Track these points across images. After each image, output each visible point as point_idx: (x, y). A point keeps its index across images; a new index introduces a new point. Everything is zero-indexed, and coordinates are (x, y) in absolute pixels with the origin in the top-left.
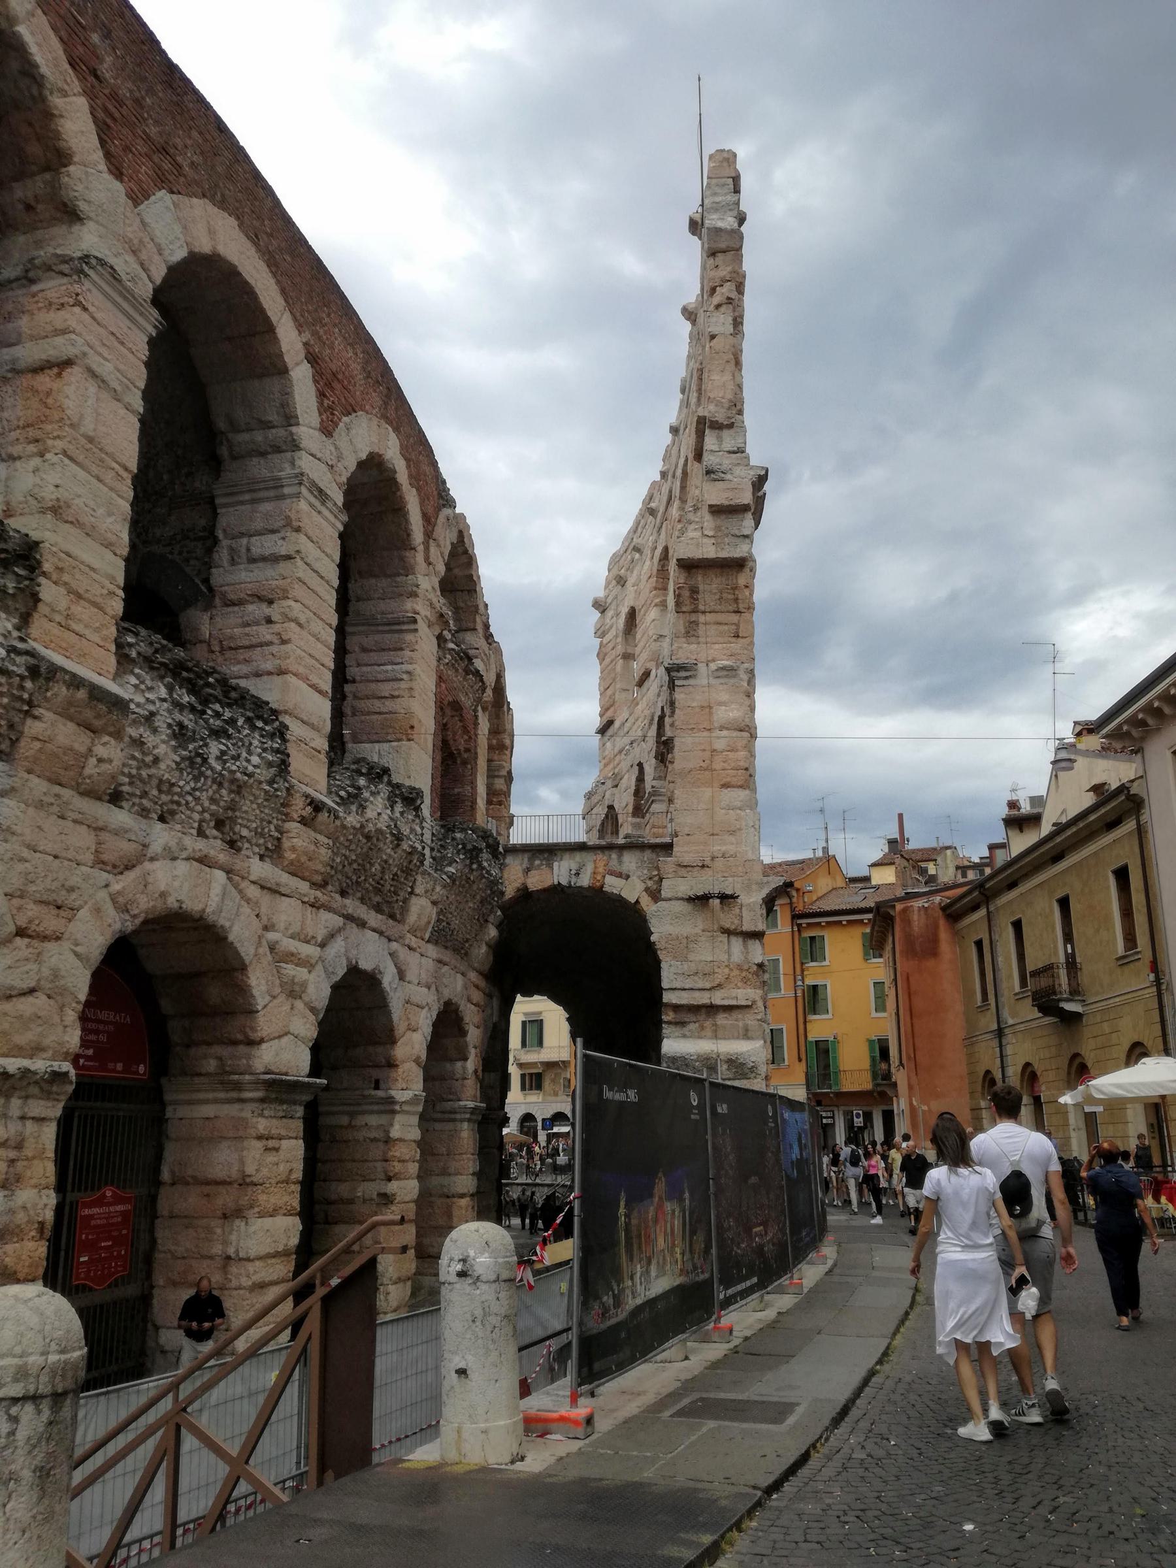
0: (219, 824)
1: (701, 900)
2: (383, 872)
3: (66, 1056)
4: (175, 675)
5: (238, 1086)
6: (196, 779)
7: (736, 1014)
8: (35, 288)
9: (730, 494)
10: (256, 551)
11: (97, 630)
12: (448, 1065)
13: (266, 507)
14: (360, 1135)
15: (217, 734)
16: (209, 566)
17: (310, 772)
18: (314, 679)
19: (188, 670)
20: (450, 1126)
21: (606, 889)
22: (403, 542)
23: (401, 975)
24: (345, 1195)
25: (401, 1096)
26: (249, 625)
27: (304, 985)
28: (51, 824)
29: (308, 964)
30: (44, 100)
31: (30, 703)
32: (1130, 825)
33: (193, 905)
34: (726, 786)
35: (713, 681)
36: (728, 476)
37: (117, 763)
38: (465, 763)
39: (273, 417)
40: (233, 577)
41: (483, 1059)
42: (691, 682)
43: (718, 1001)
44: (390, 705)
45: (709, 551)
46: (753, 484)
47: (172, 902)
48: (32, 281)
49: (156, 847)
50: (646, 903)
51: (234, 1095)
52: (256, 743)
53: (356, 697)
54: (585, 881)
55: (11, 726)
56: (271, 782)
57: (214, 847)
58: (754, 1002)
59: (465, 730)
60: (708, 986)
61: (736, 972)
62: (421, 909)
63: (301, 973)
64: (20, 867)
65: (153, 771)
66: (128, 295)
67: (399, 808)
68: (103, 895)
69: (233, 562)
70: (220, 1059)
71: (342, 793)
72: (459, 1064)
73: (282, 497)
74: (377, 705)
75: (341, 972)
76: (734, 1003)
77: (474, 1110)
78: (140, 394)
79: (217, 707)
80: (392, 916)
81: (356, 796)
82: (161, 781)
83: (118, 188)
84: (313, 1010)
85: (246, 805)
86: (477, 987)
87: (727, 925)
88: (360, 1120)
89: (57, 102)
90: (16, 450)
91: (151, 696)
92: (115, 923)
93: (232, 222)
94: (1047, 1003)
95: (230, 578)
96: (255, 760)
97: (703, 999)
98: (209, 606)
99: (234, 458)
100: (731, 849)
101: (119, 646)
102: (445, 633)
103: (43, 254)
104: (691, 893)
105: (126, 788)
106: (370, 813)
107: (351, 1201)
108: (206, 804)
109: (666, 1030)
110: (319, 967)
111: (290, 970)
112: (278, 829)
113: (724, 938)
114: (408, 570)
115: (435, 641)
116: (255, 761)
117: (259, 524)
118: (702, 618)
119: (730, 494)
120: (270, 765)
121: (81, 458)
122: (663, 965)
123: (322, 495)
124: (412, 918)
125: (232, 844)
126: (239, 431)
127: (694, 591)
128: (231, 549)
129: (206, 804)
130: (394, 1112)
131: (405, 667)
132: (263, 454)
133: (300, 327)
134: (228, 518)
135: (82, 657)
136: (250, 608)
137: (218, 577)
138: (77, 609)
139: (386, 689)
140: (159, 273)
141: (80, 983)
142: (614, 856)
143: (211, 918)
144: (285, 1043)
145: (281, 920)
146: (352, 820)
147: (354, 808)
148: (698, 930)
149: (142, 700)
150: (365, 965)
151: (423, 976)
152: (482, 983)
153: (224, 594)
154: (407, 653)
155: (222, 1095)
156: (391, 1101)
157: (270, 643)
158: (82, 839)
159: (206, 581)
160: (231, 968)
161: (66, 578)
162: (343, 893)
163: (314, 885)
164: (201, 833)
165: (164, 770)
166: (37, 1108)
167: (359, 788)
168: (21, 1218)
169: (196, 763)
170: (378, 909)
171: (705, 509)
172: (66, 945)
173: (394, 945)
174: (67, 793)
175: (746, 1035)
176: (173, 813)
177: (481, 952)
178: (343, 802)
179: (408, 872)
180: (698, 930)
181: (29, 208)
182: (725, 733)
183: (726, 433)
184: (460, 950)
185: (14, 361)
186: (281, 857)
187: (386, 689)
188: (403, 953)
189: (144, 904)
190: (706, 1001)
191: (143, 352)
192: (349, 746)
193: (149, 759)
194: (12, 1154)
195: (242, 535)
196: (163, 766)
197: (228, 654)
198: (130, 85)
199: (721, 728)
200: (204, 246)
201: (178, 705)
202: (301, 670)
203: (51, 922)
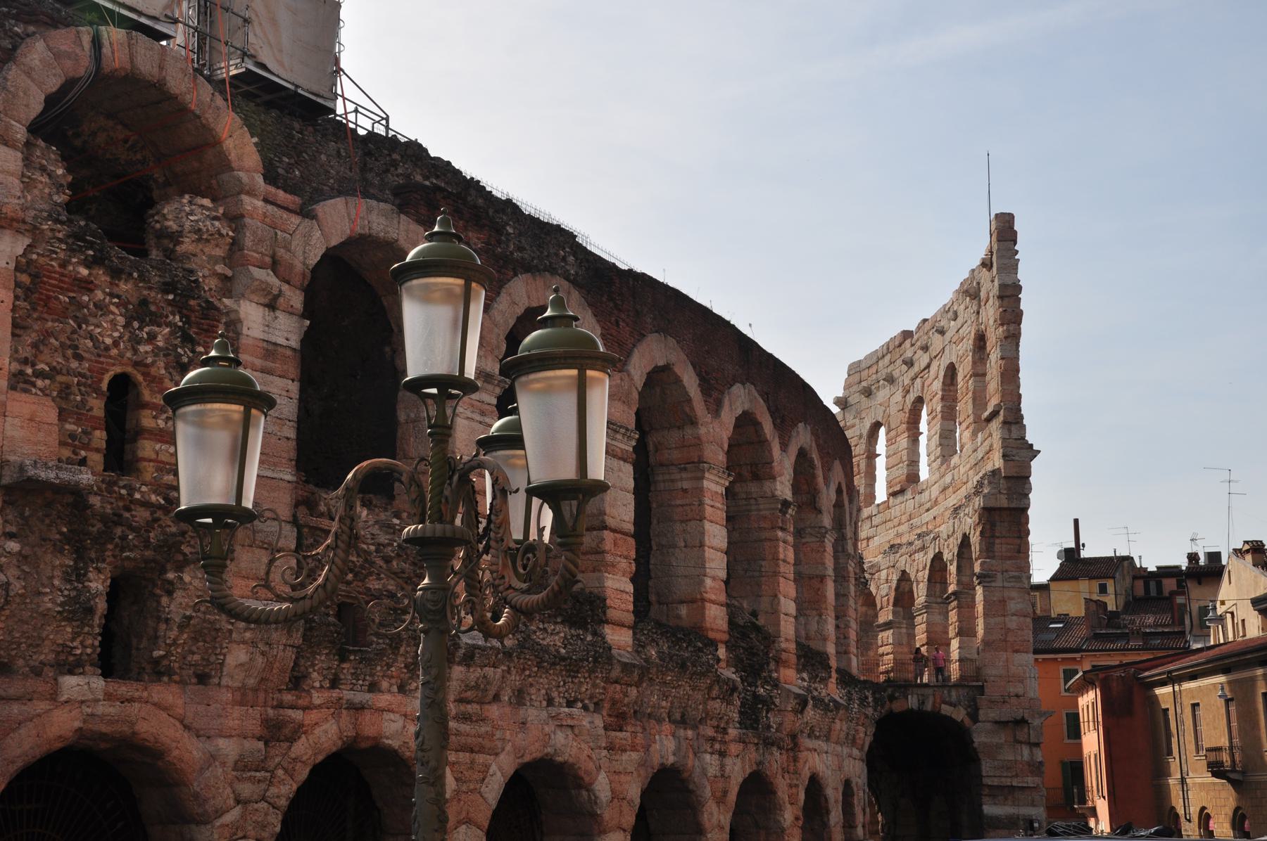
21: (943, 712)
34: (1017, 651)
43: (1015, 784)
50: (967, 722)
97: (1007, 782)
100: (1020, 691)
104: (997, 719)
109: (985, 799)
118: (997, 541)
148: (1002, 741)
175: (1033, 805)
199: (1013, 615)
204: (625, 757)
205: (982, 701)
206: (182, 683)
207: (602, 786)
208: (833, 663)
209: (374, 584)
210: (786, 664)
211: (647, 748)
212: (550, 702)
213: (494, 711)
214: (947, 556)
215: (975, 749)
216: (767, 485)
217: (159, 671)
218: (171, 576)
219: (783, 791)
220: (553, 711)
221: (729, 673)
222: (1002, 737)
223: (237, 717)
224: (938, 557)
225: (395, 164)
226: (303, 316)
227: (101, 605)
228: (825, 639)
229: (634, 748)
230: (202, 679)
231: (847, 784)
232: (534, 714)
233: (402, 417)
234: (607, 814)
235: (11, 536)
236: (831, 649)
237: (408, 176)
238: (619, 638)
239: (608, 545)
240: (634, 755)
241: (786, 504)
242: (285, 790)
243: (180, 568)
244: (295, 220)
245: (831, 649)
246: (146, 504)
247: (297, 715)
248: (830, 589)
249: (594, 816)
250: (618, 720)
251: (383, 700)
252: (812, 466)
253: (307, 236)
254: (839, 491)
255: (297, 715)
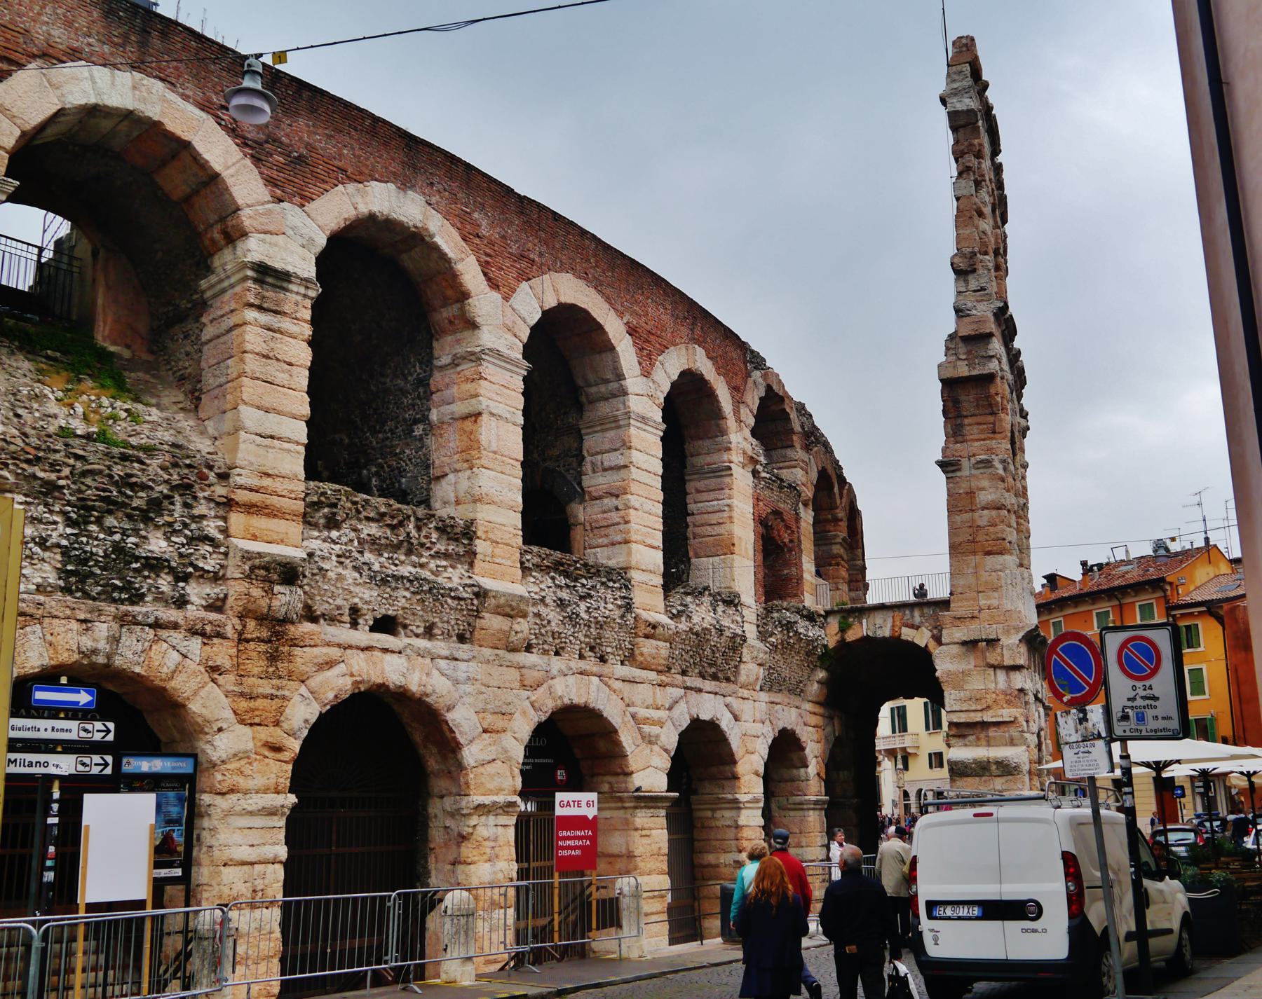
0: (592, 649)
1: (970, 645)
2: (714, 653)
3: (515, 792)
4: (556, 570)
5: (621, 800)
6: (574, 626)
7: (1003, 728)
8: (459, 369)
9: (975, 326)
10: (606, 464)
11: (509, 558)
12: (795, 771)
13: (611, 434)
14: (719, 823)
15: (582, 598)
16: (580, 474)
17: (650, 602)
18: (649, 541)
19: (562, 565)
20: (801, 813)
21: (903, 637)
22: (718, 414)
23: (736, 718)
24: (713, 862)
25: (742, 797)
26: (605, 512)
27: (658, 736)
28: (496, 671)
29: (660, 724)
30: (452, 268)
31: (477, 611)
33: (579, 700)
34: (989, 553)
35: (974, 472)
36: (974, 312)
37: (526, 631)
38: (790, 551)
39: (609, 376)
40: (594, 481)
41: (826, 765)
42: (958, 474)
44: (718, 530)
46: (995, 315)
47: (566, 701)
48: (457, 365)
49: (554, 672)
51: (620, 805)
52: (609, 596)
53: (695, 526)
54: (886, 632)
55: (469, 625)
56: (622, 617)
57: (591, 664)
58: (1016, 718)
59: (787, 527)
60: (979, 708)
61: (1001, 697)
62: (750, 670)
63: (655, 730)
64: (482, 697)
65: (548, 628)
66: (508, 360)
67: (720, 608)
68: (527, 703)
69: (594, 472)
70: (610, 783)
71: (674, 611)
72: (802, 770)
73: (619, 427)
74: (709, 530)
75: (686, 723)
76: (1000, 719)
77: (816, 802)
78: (521, 413)
79: (584, 581)
80: (728, 680)
81: (683, 611)
82: (553, 633)
83: (496, 296)
84: (666, 751)
85: (607, 634)
86: (815, 714)
87: (992, 662)
88: (718, 814)
89: (459, 267)
90: (458, 466)
91: (543, 586)
92: (535, 718)
93: (570, 276)
95: (593, 482)
96: (610, 606)
97: (977, 717)
98: (582, 501)
99: (591, 402)
100: (994, 602)
101: (522, 563)
102: (759, 467)
103: (460, 350)
105: (534, 641)
106: (696, 619)
107: (717, 866)
108: (583, 639)
110: (669, 724)
111: (647, 729)
112: (630, 643)
113: (991, 671)
114: (723, 432)
115: (750, 475)
116: (609, 607)
117: (607, 446)
118: (966, 421)
119: (975, 326)
120: (620, 607)
121: (491, 466)
122: (946, 694)
123: (644, 420)
124: (743, 678)
125: (603, 659)
126: (591, 386)
128: (592, 463)
129: (583, 639)
130: (740, 808)
131: (727, 502)
132: (607, 399)
133: (621, 314)
134: (590, 442)
135: (502, 576)
136: (606, 501)
137: (587, 481)
138: (498, 551)
139: (714, 518)
140: (525, 334)
141: (519, 753)
142: (907, 612)
143: (591, 706)
144: (650, 772)
145: (638, 699)
146: (683, 625)
147: (683, 619)
149: (537, 590)
150: (705, 716)
151: (757, 715)
152: (818, 709)
153: (590, 492)
154: (727, 491)
155: (613, 805)
156: (736, 801)
157: (618, 524)
158: (514, 674)
159: (580, 484)
160: (609, 732)
161: (490, 535)
162: (684, 673)
163: (659, 672)
164: (581, 657)
165: (554, 626)
166: (503, 820)
167: (686, 605)
168: (500, 876)
169: (573, 619)
170: (715, 677)
171: (958, 339)
172: (509, 734)
173: (728, 699)
174: (501, 652)
175: (1012, 743)
176: (563, 648)
177: (814, 688)
178: (674, 617)
179: (734, 649)
180: (971, 667)
181: (451, 322)
182: (986, 512)
183: (970, 277)
184: (796, 690)
185: (452, 413)
186: (634, 660)
187: (714, 518)
188: (736, 703)
189: (549, 706)
190: (979, 719)
191: (520, 386)
192: (693, 560)
193: (545, 622)
194: (492, 844)
195: (598, 453)
196: (553, 624)
197: (596, 531)
198: (498, 230)
199: (983, 508)
200: (551, 303)
201: (561, 587)
202: (639, 538)
203: (500, 723)
215: (937, 679)
222: (968, 664)
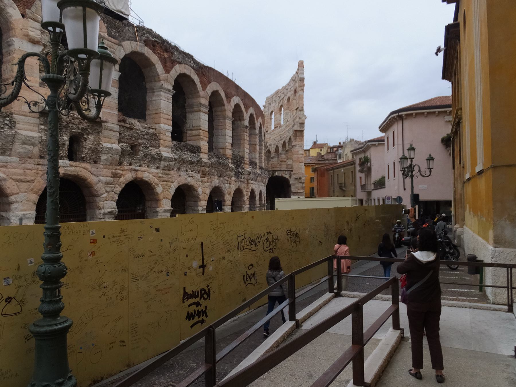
1: (296, 179)
32: (353, 166)
45: (299, 129)
54: (280, 175)
94: (341, 188)
127: (296, 134)
204: (206, 184)
205: (292, 173)
206: (90, 163)
207: (200, 190)
208: (258, 164)
209: (140, 141)
210: (246, 164)
211: (211, 182)
212: (187, 171)
213: (172, 172)
214: (286, 141)
216: (242, 122)
217: (83, 160)
218: (85, 136)
219: (245, 193)
220: (187, 173)
221: (231, 165)
222: (296, 182)
223: (105, 172)
224: (284, 142)
225: (144, 34)
226: (119, 72)
227: (67, 143)
228: (256, 159)
229: (208, 182)
230: (95, 162)
231: (261, 191)
232: (182, 173)
233: (148, 99)
234: (201, 197)
235: (42, 124)
236: (257, 161)
237: (148, 37)
238: (204, 157)
239: (201, 134)
240: (208, 184)
241: (247, 127)
242: (119, 189)
243: (88, 134)
244: (116, 46)
245: (257, 161)
246: (78, 118)
247: (121, 172)
248: (258, 147)
249: (198, 197)
250: (204, 175)
251: (143, 169)
252: (254, 118)
253: (120, 51)
254: (261, 124)
255: (121, 172)
